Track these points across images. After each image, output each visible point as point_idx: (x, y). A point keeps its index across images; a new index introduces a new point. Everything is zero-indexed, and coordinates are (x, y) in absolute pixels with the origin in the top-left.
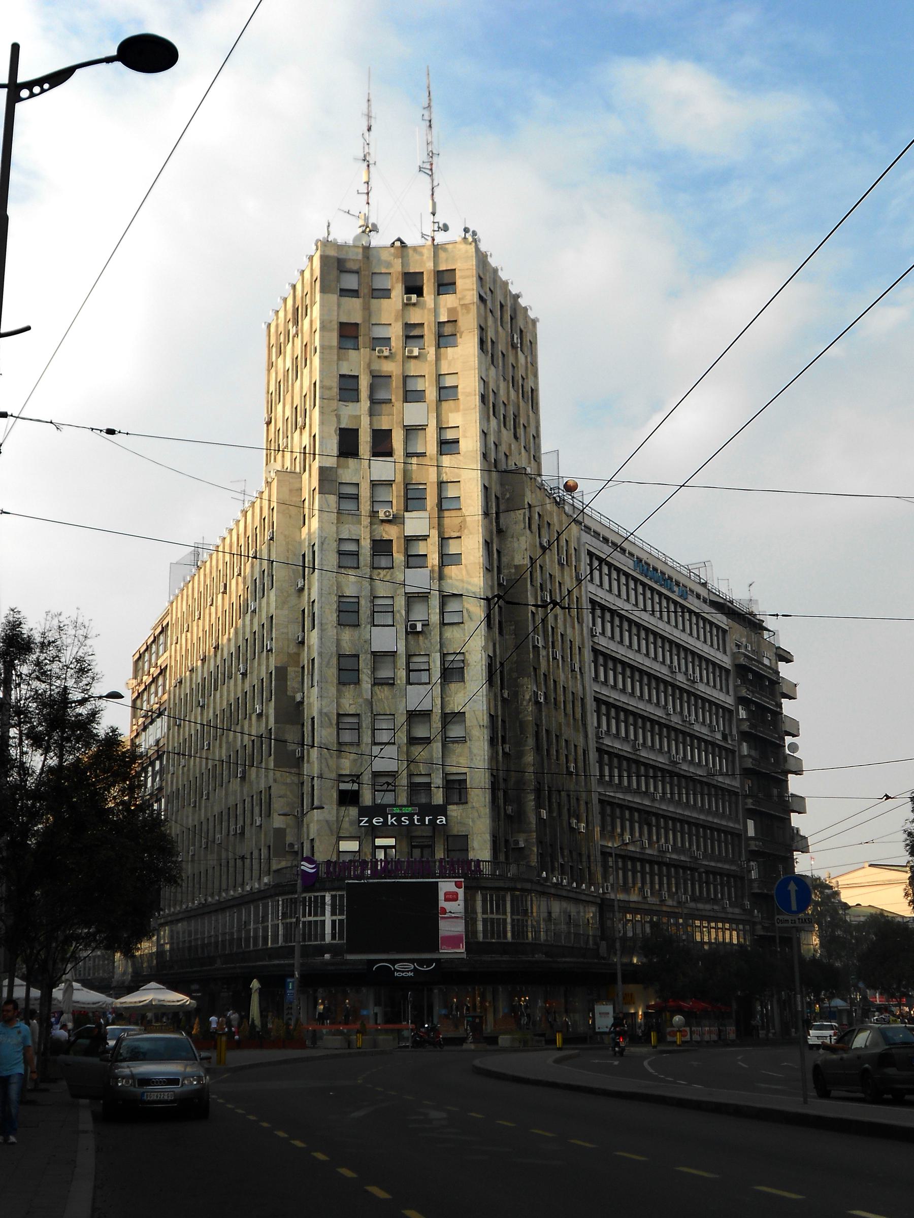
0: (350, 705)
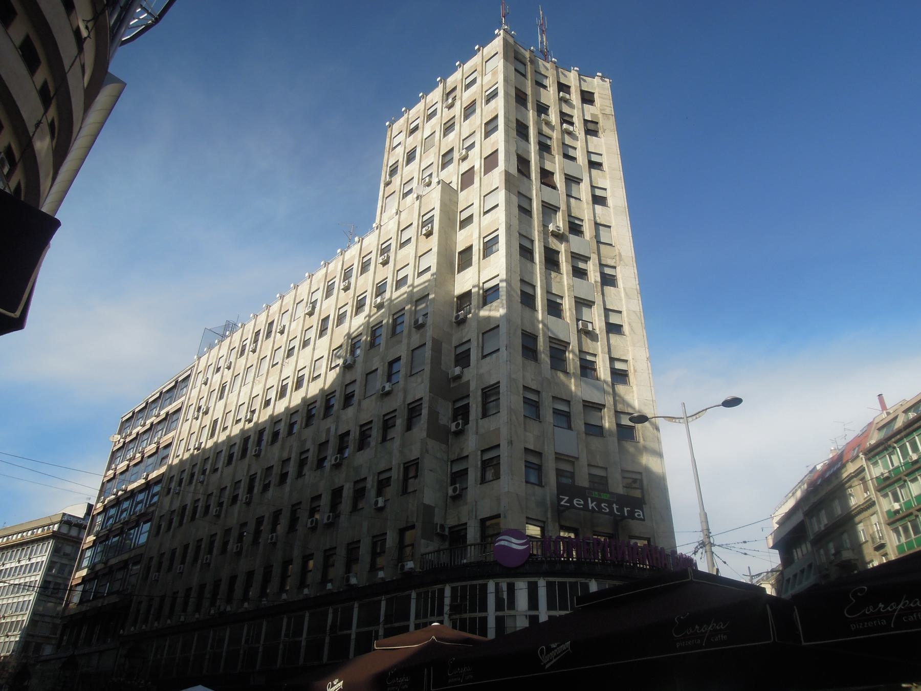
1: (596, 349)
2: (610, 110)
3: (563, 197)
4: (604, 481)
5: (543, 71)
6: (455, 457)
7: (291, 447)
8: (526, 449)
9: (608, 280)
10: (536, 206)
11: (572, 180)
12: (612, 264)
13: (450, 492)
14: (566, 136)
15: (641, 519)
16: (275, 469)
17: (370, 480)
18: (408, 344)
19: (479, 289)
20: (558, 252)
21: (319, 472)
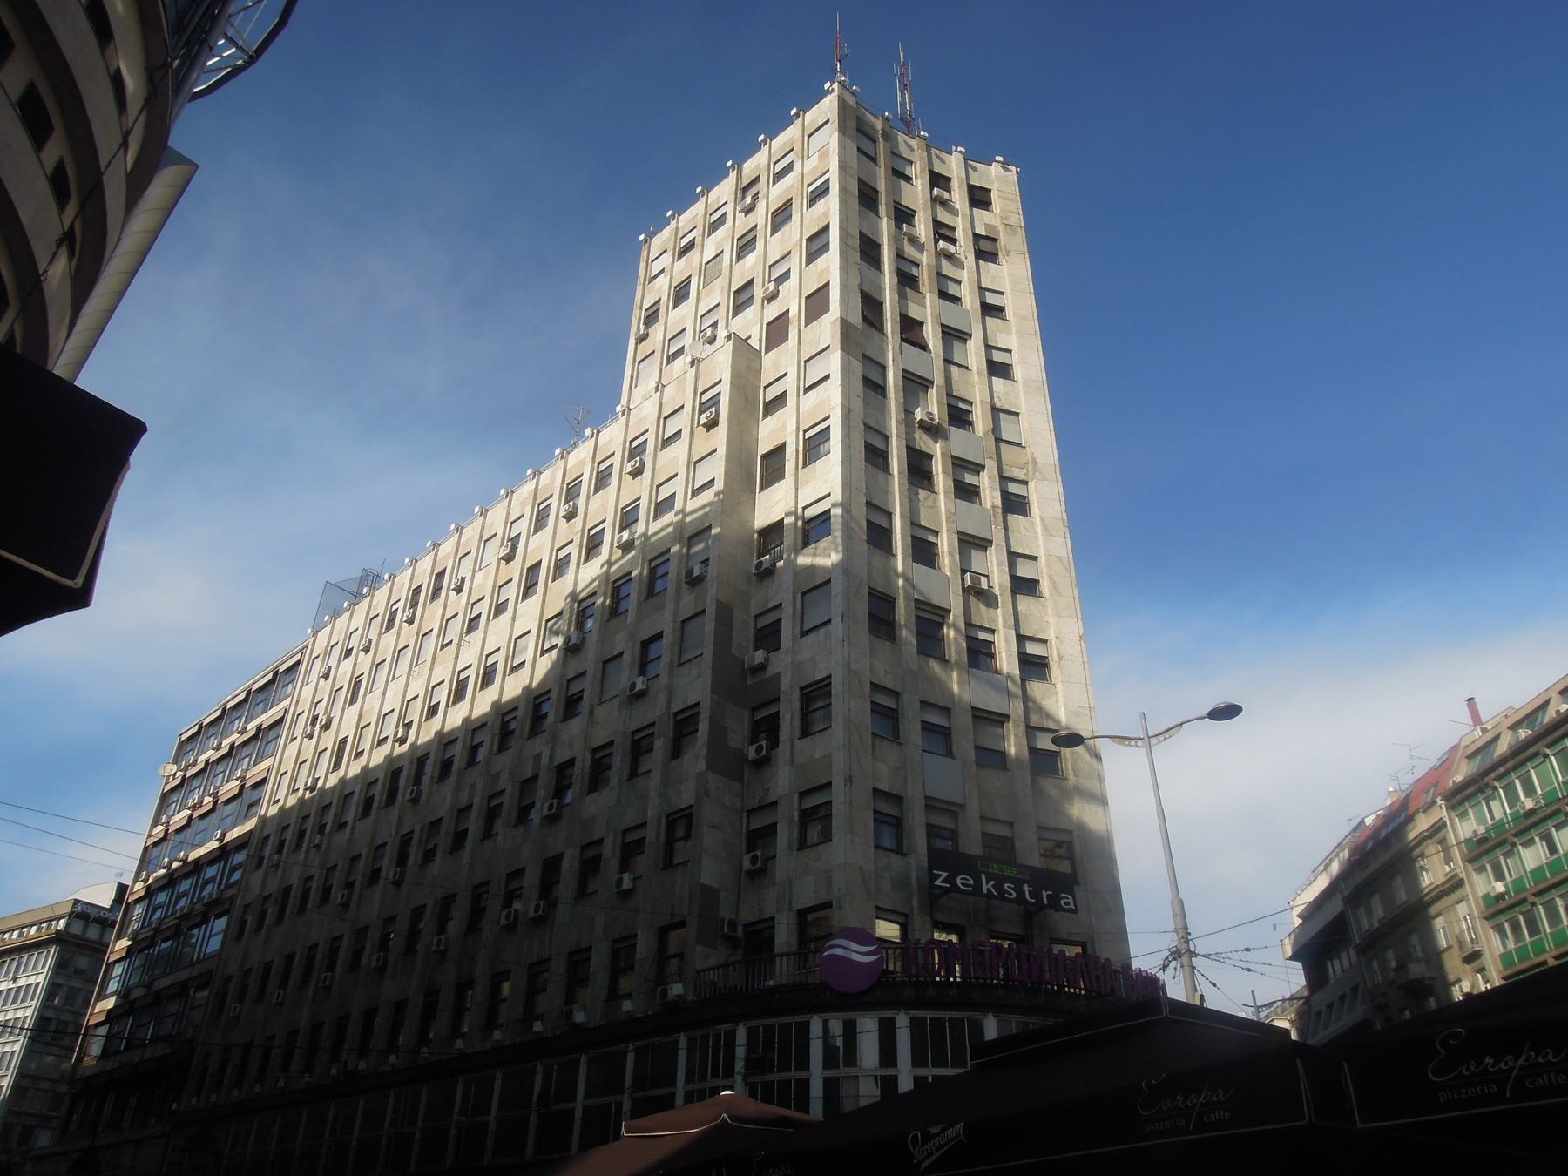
0: (886, 673)
1: (995, 621)
2: (1017, 218)
3: (939, 364)
4: (1008, 844)
5: (905, 153)
6: (755, 803)
7: (473, 786)
8: (875, 790)
9: (1014, 504)
10: (892, 378)
11: (953, 336)
12: (1022, 477)
13: (747, 864)
14: (944, 262)
15: (1070, 910)
16: (445, 824)
17: (608, 842)
18: (676, 612)
19: (797, 519)
20: (930, 457)
21: (521, 829)
